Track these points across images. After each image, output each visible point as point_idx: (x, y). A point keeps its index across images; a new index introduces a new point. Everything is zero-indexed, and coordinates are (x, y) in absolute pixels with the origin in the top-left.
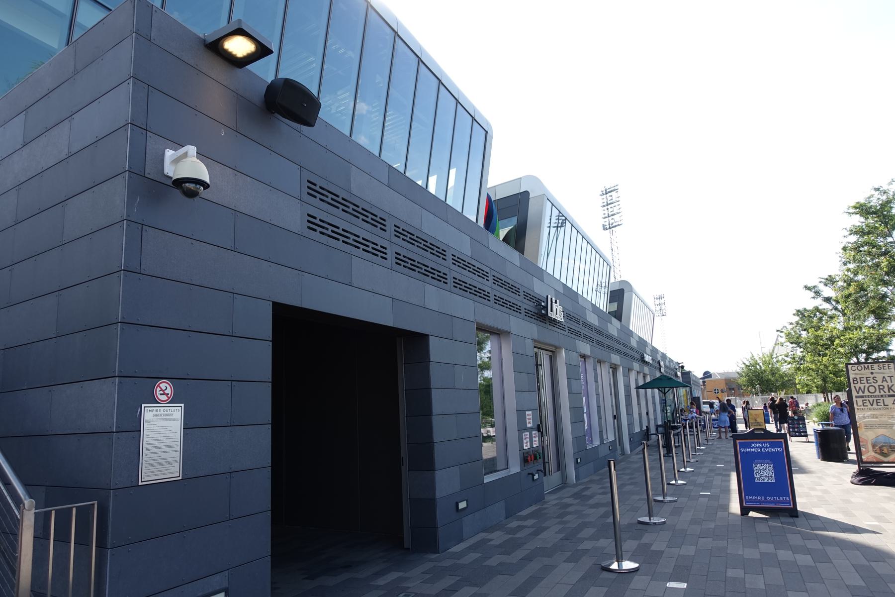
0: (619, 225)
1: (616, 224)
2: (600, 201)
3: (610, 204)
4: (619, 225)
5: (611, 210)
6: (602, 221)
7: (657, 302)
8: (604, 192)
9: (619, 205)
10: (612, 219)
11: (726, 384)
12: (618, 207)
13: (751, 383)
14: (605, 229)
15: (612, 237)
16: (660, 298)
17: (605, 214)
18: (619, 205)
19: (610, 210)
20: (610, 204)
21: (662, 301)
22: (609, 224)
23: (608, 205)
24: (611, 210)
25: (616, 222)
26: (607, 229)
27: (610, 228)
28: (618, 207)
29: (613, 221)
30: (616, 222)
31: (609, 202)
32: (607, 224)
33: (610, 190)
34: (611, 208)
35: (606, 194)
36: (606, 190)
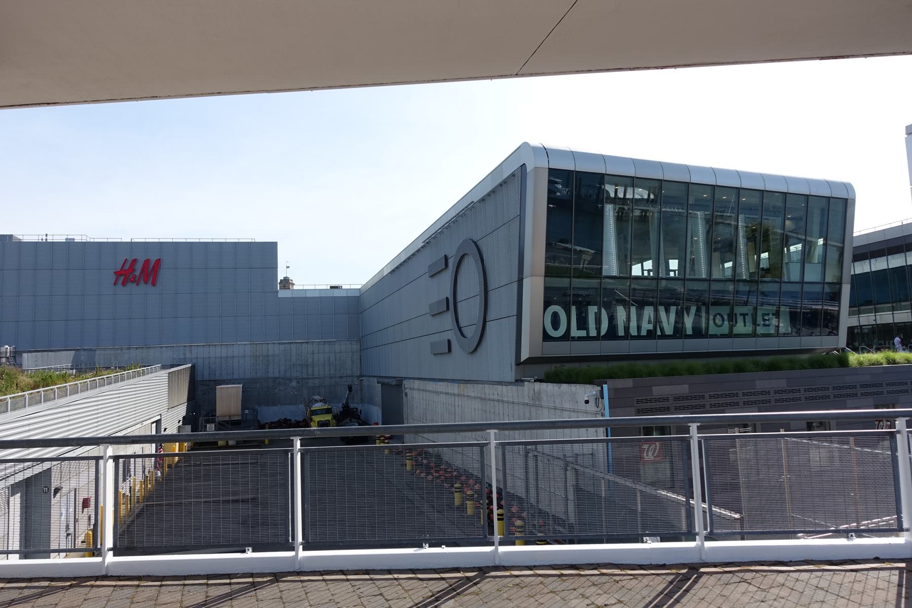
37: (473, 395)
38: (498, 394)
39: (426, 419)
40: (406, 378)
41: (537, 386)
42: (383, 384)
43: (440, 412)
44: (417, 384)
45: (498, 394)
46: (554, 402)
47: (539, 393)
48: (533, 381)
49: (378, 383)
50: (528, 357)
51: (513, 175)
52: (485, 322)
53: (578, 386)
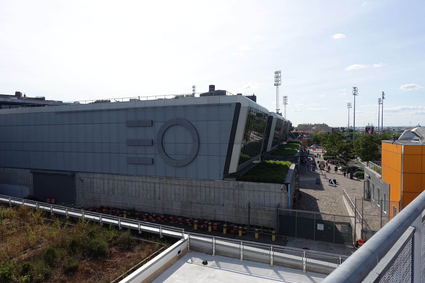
0: (280, 85)
1: (279, 84)
2: (274, 75)
3: (278, 77)
4: (280, 85)
5: (278, 79)
6: (274, 83)
7: (284, 99)
8: (276, 73)
9: (281, 78)
10: (278, 82)
11: (308, 140)
12: (280, 79)
13: (314, 141)
14: (275, 85)
15: (277, 89)
16: (286, 97)
17: (275, 80)
18: (281, 78)
19: (277, 79)
20: (278, 77)
21: (286, 98)
22: (277, 84)
23: (277, 77)
24: (278, 79)
25: (279, 83)
26: (276, 85)
27: (277, 85)
28: (280, 79)
29: (278, 83)
30: (279, 83)
31: (277, 76)
32: (276, 83)
33: (278, 72)
34: (278, 78)
35: (277, 73)
36: (277, 72)
37: (178, 183)
38: (205, 184)
39: (114, 193)
40: (79, 172)
41: (241, 183)
42: (34, 173)
43: (135, 190)
44: (98, 176)
45: (205, 184)
46: (254, 188)
47: (242, 185)
48: (235, 180)
49: (31, 172)
50: (235, 172)
51: (230, 105)
52: (196, 155)
53: (271, 184)
